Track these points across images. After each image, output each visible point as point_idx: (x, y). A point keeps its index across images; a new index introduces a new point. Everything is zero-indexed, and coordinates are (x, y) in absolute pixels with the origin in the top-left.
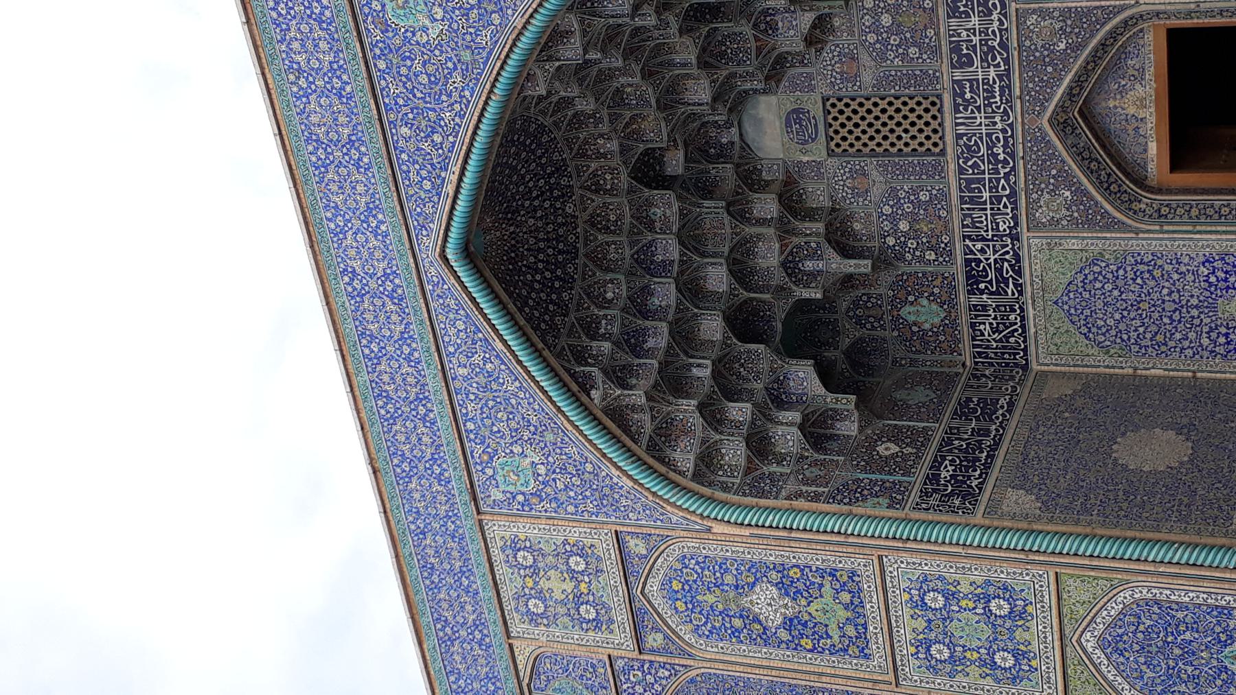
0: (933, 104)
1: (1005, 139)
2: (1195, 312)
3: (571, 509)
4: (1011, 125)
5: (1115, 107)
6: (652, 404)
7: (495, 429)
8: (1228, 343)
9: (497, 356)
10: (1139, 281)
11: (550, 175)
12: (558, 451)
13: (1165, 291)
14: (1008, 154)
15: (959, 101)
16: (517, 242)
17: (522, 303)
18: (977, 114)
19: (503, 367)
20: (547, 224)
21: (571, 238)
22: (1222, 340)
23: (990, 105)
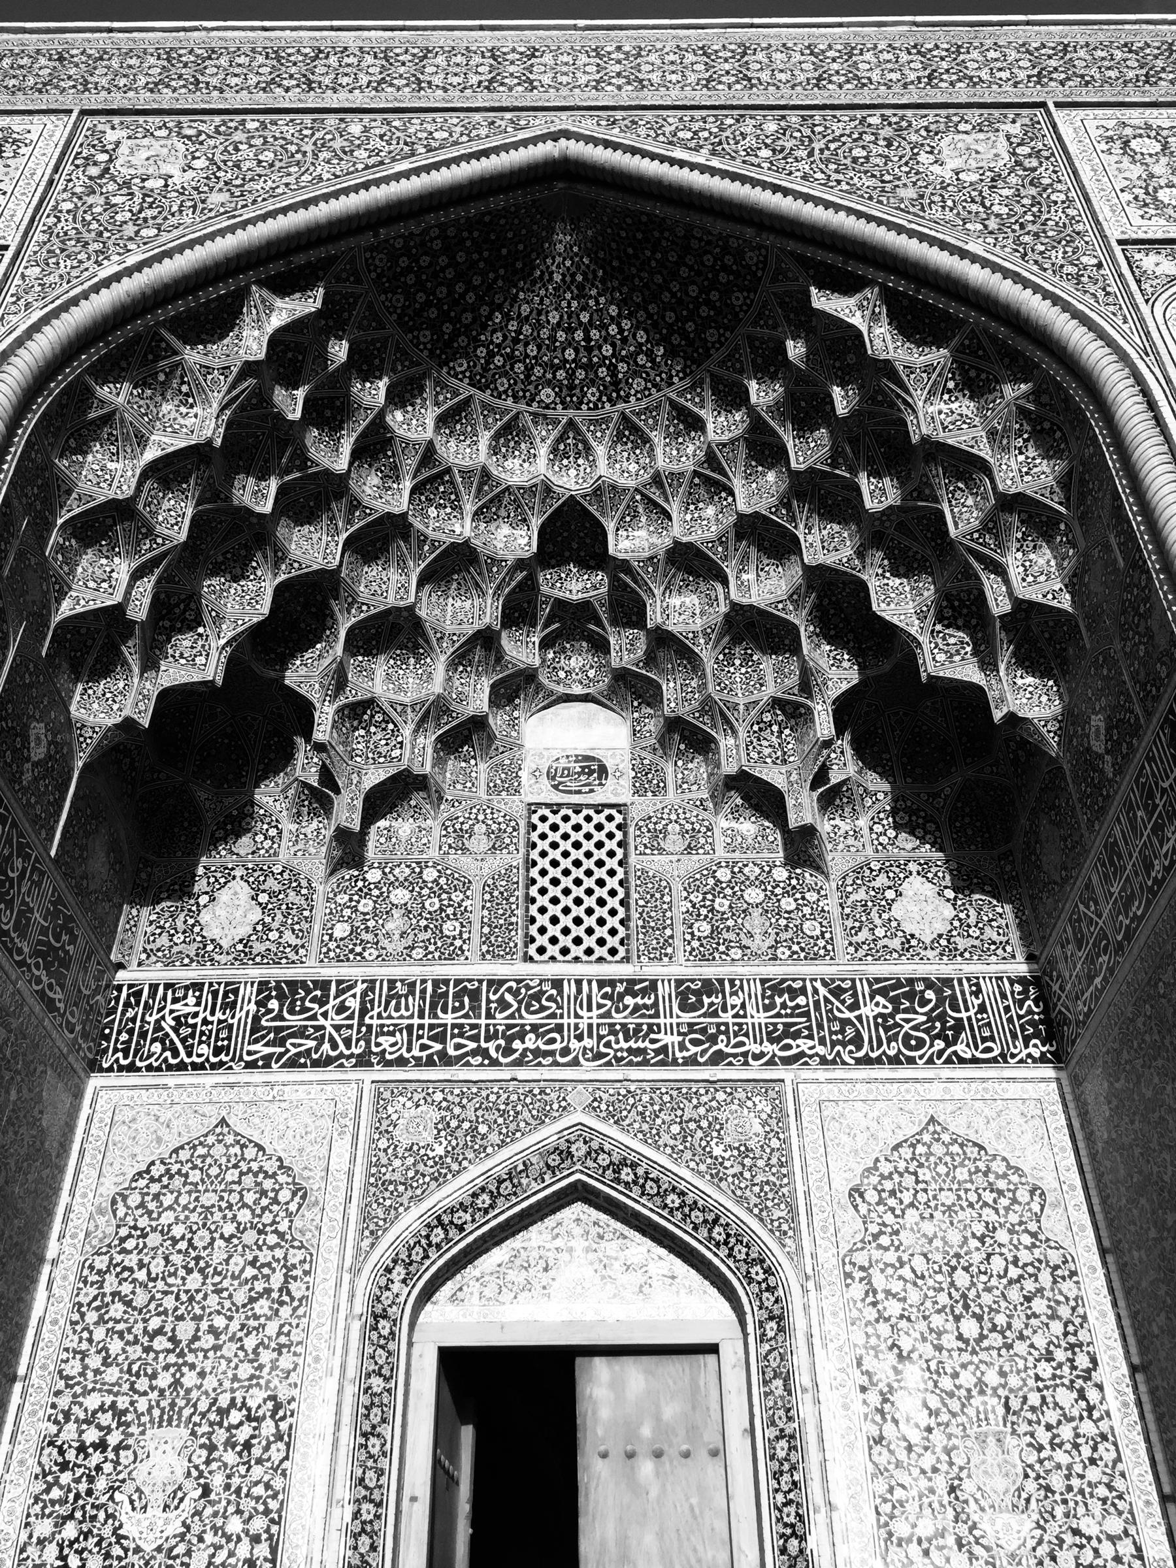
0: (613, 952)
1: (552, 1053)
2: (164, 1380)
3: (68, 206)
5: (570, 1250)
6: (235, 370)
8: (82, 1449)
9: (382, 163)
10: (250, 1272)
13: (220, 1322)
15: (620, 988)
16: (534, 283)
18: (595, 1012)
19: (360, 166)
20: (539, 347)
21: (503, 384)
22: (92, 1435)
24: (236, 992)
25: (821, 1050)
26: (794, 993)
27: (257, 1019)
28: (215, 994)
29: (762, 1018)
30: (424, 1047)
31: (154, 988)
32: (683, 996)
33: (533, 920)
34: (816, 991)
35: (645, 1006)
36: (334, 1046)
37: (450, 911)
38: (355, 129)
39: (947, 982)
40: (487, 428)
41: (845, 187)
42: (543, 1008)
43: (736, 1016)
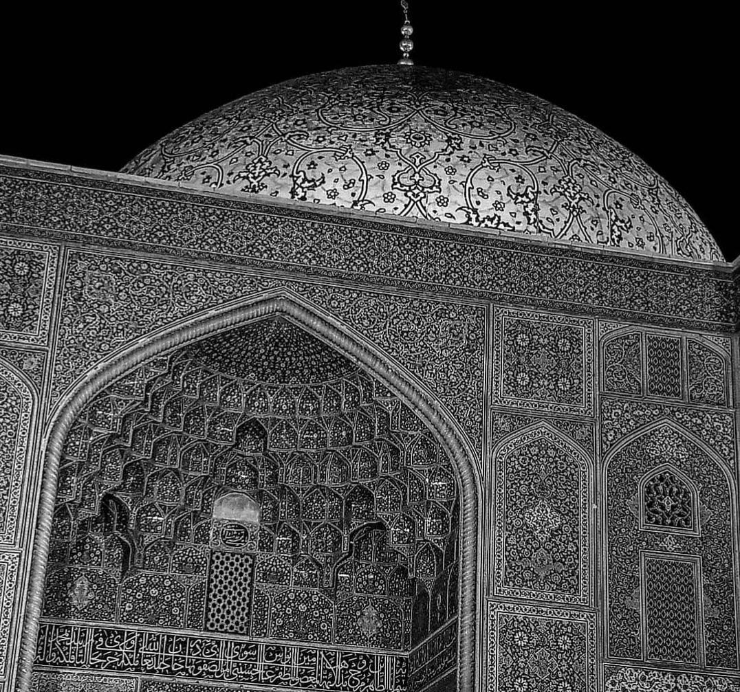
0: (242, 629)
1: (213, 673)
4: (222, 678)
7: (141, 285)
11: (284, 372)
12: (120, 327)
14: (202, 673)
15: (243, 647)
17: (223, 334)
19: (194, 309)
20: (253, 360)
23: (238, 666)
24: (85, 632)
25: (317, 682)
26: (312, 656)
27: (94, 646)
28: (77, 632)
29: (296, 666)
30: (162, 666)
31: (51, 627)
32: (268, 652)
33: (210, 610)
34: (320, 656)
35: (252, 656)
36: (126, 662)
37: (175, 602)
38: (191, 277)
39: (372, 657)
40: (222, 385)
41: (395, 354)
42: (211, 653)
43: (287, 664)
